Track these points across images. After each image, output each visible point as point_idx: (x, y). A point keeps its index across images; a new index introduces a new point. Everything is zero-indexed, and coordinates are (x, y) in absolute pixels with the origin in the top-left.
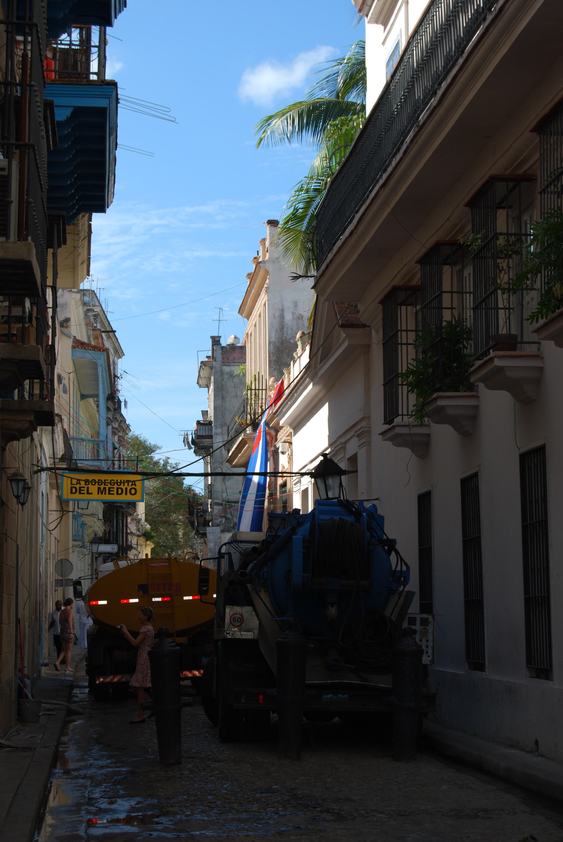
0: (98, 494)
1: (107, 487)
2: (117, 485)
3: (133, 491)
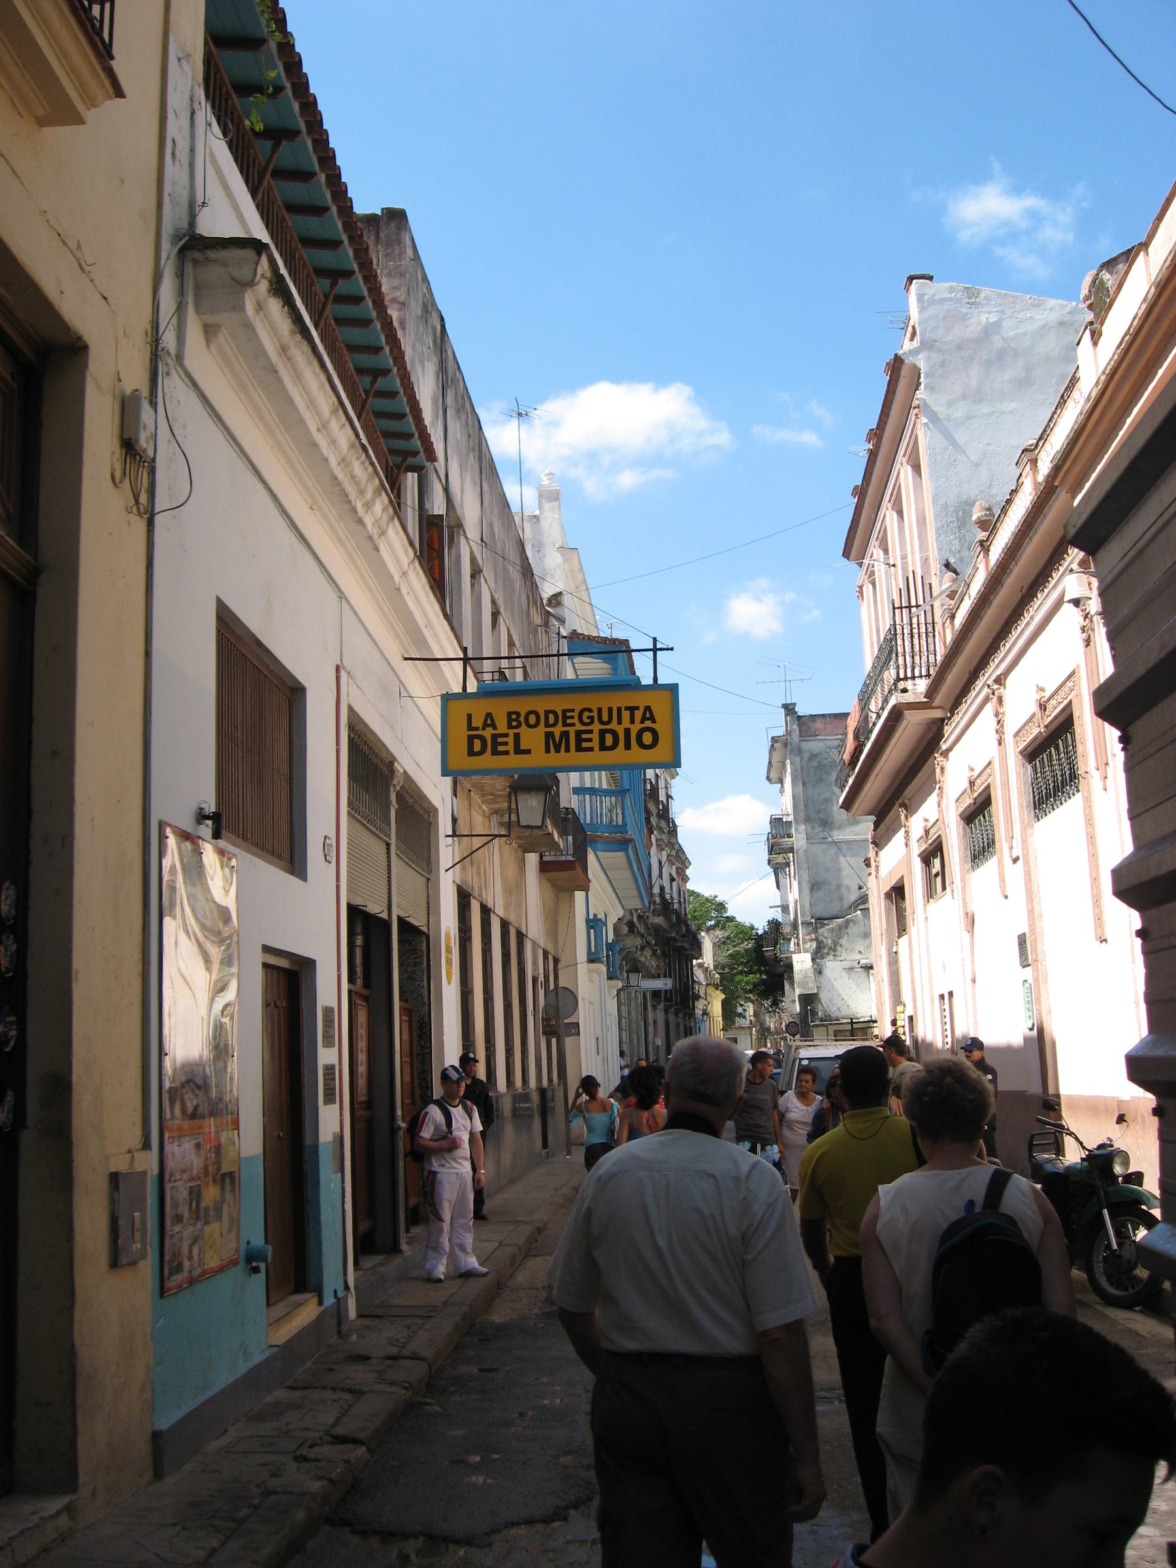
0: (548, 751)
1: (572, 730)
3: (647, 738)
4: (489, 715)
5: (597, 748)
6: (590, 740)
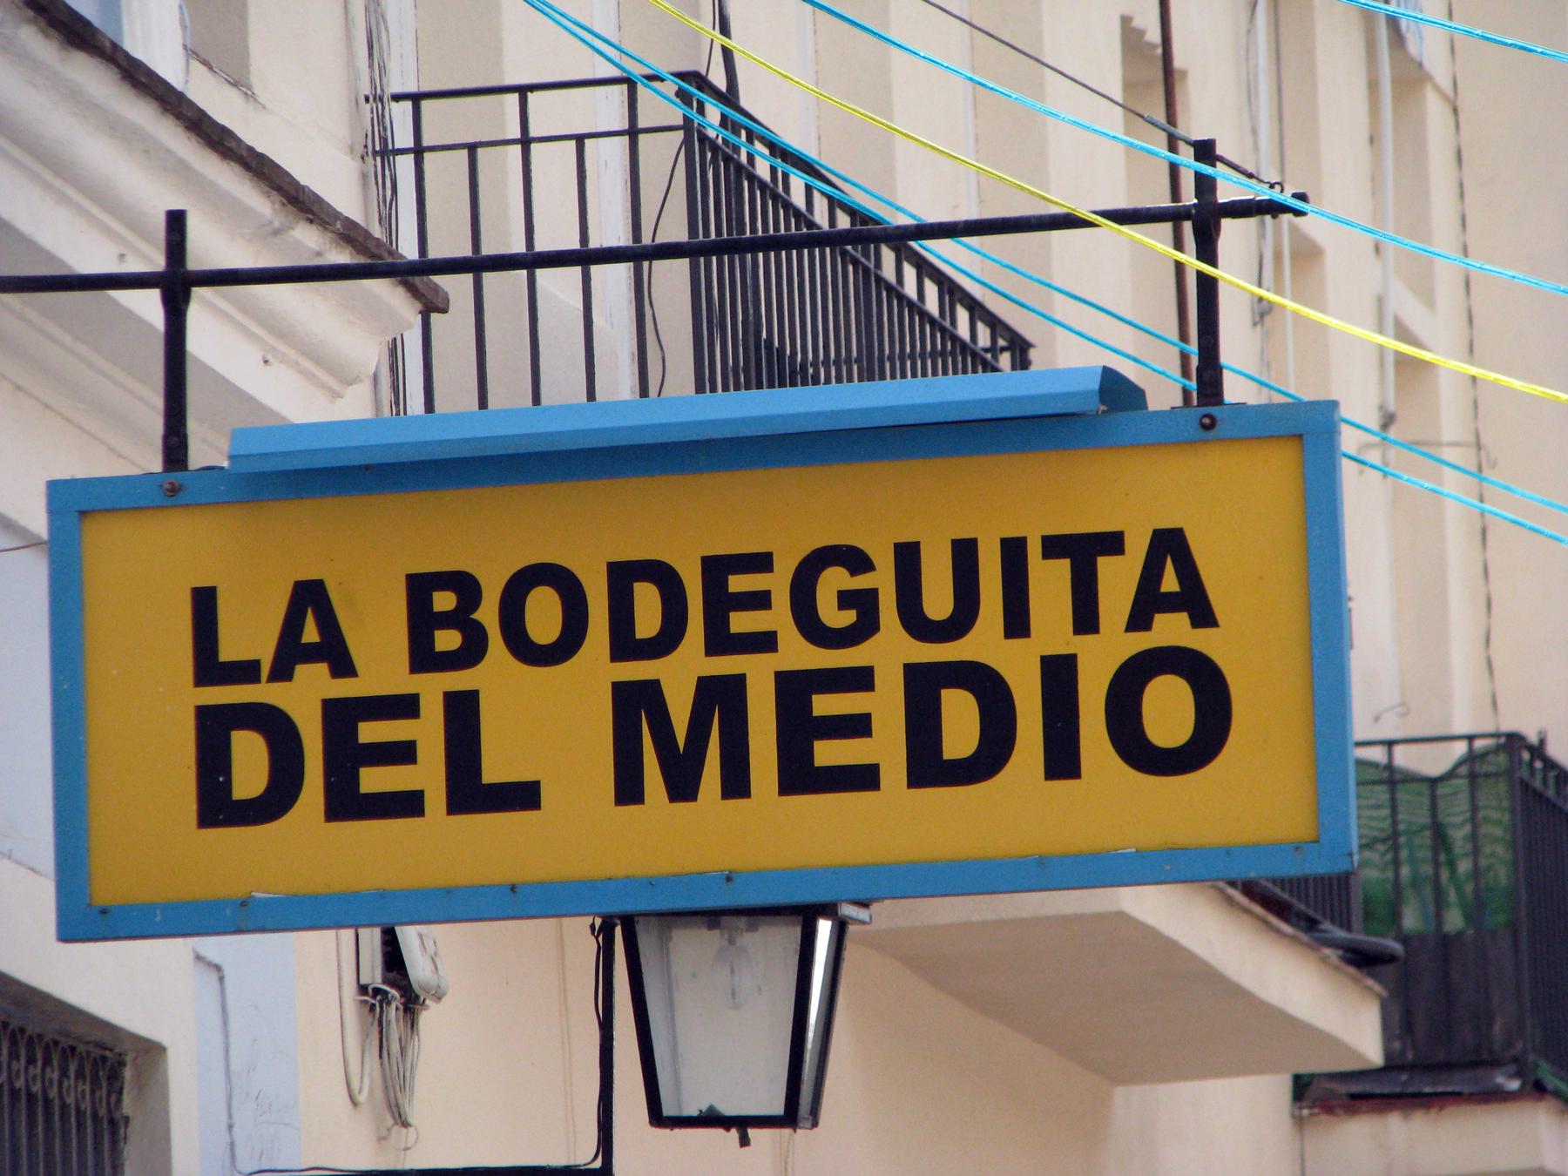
0: (629, 790)
1: (759, 673)
2: (917, 624)
5: (894, 769)
6: (858, 726)
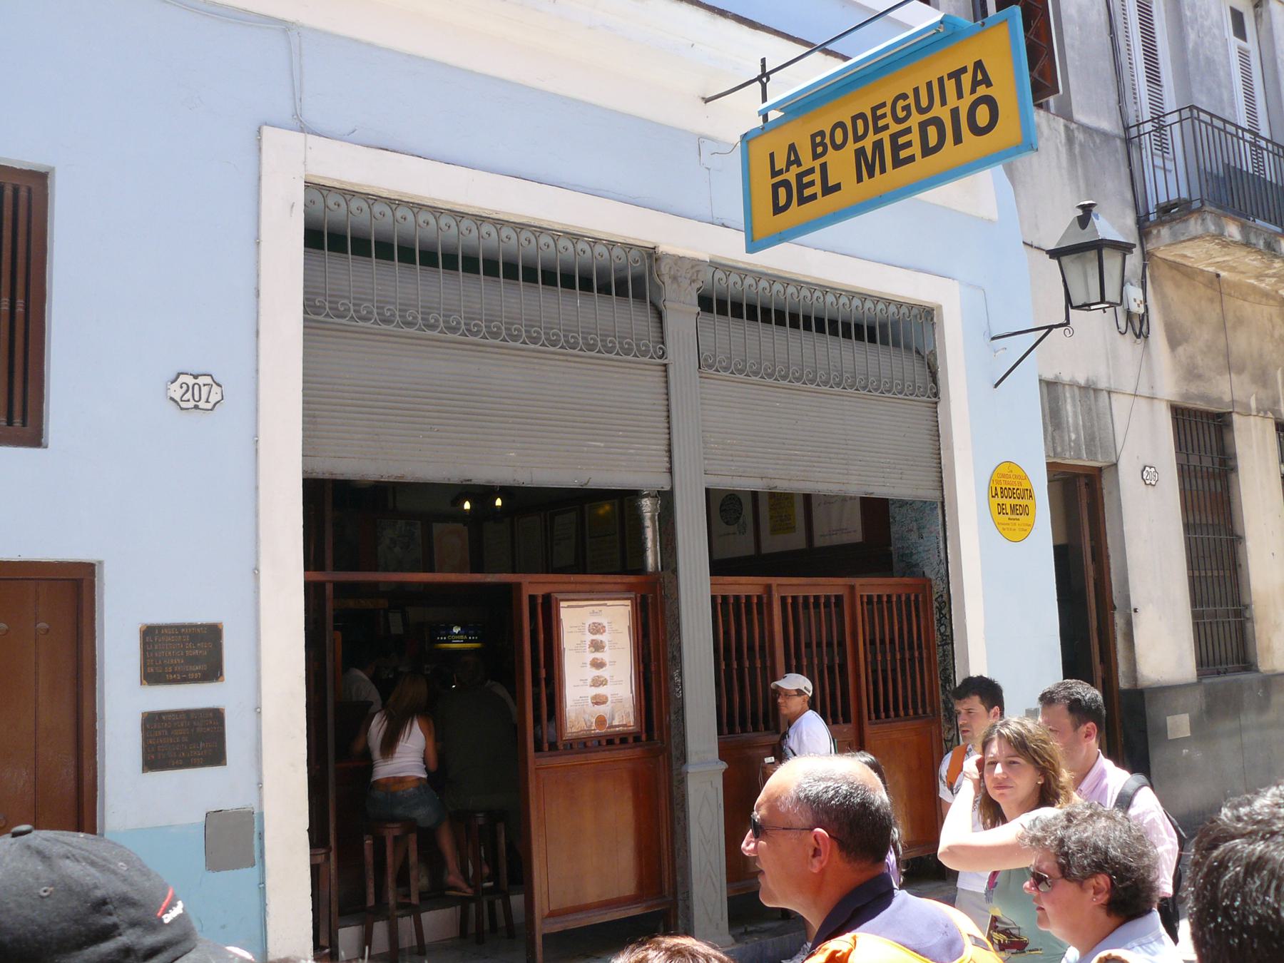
0: (860, 179)
1: (885, 136)
2: (921, 111)
4: (792, 148)
